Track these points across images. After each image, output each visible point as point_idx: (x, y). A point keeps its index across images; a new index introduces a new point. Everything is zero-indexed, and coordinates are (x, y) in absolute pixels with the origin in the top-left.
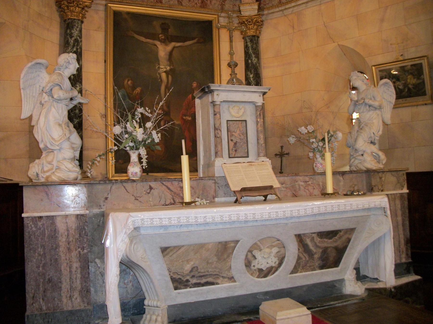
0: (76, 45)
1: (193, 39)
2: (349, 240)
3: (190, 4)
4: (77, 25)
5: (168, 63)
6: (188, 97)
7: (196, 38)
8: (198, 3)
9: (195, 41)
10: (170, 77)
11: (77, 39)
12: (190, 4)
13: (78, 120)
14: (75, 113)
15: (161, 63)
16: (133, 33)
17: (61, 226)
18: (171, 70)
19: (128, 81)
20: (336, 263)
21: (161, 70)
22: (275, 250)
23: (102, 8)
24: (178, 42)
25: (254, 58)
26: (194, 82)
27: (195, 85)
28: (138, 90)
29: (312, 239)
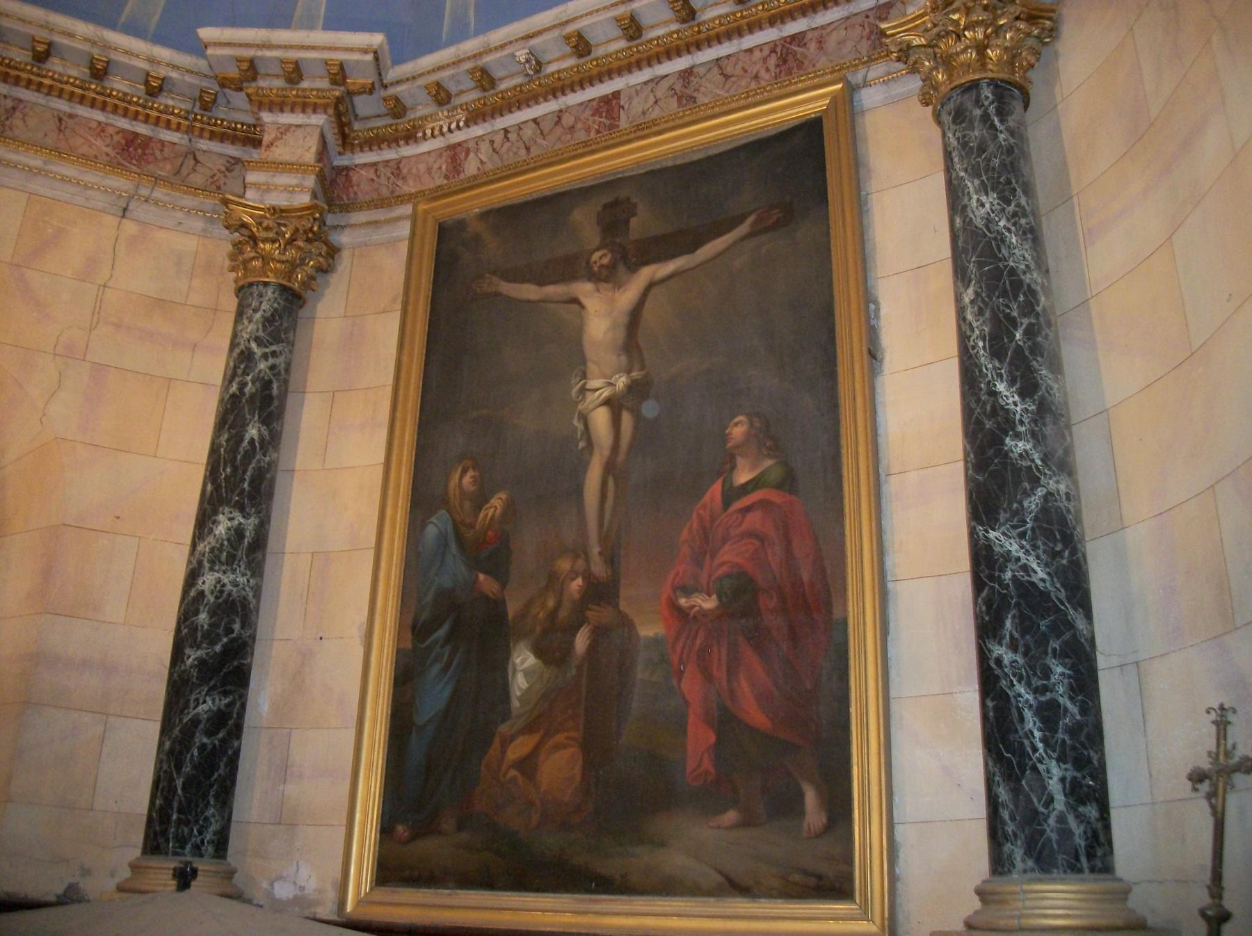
0: (240, 371)
3: (728, 91)
4: (254, 304)
5: (624, 359)
6: (707, 498)
7: (751, 213)
8: (763, 74)
9: (743, 229)
11: (249, 349)
12: (728, 91)
13: (199, 653)
14: (192, 622)
15: (592, 367)
16: (495, 279)
18: (631, 388)
19: (464, 472)
21: (591, 397)
25: (975, 197)
26: (734, 416)
27: (738, 431)
28: (497, 503)
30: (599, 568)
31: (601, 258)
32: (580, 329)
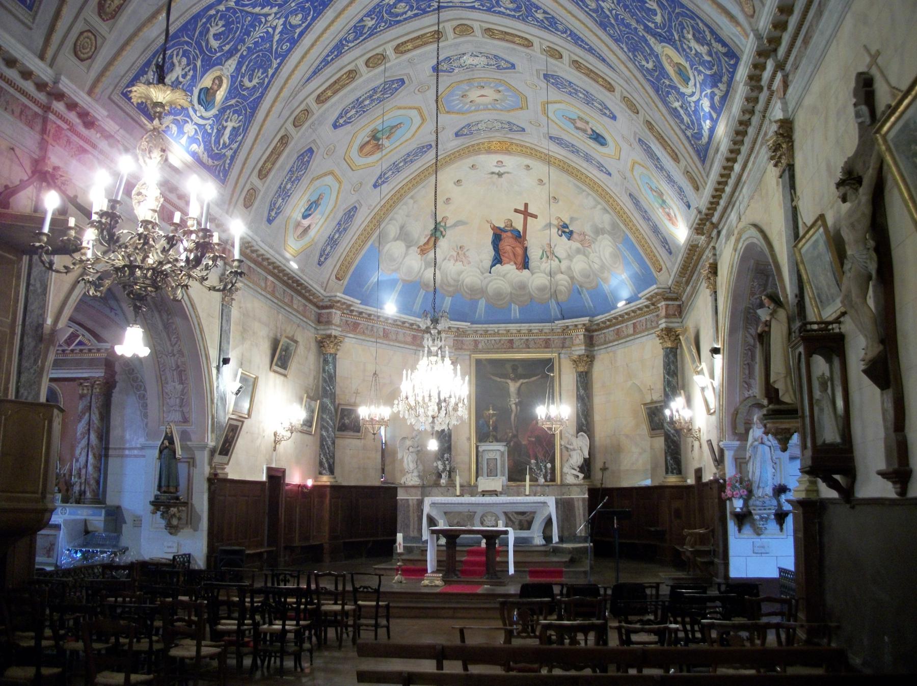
1: (539, 374)
2: (533, 518)
9: (539, 376)
10: (518, 408)
17: (410, 502)
18: (520, 402)
20: (529, 528)
22: (494, 518)
23: (467, 357)
24: (525, 379)
29: (512, 515)
30: (515, 432)
31: (512, 376)
32: (509, 389)
